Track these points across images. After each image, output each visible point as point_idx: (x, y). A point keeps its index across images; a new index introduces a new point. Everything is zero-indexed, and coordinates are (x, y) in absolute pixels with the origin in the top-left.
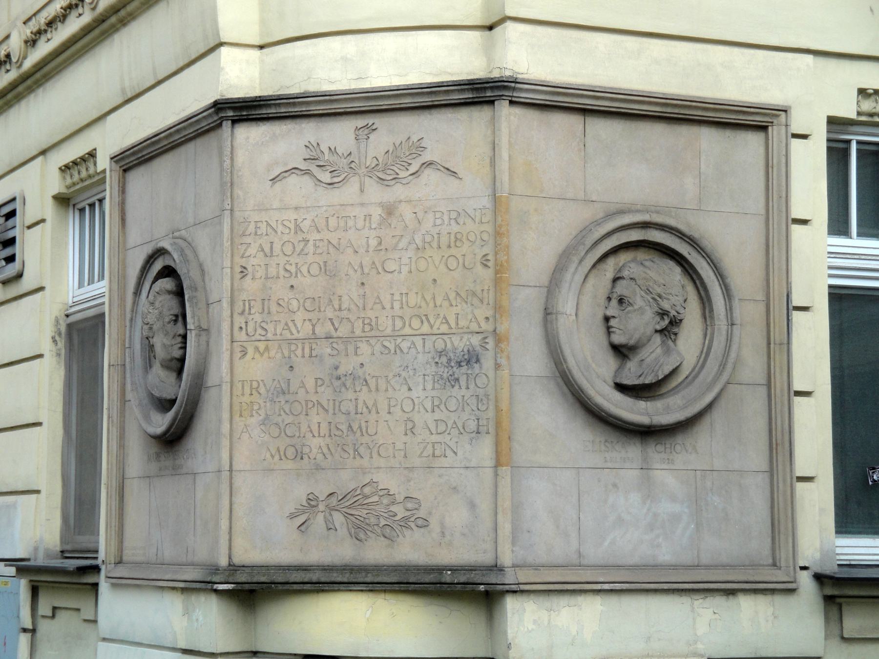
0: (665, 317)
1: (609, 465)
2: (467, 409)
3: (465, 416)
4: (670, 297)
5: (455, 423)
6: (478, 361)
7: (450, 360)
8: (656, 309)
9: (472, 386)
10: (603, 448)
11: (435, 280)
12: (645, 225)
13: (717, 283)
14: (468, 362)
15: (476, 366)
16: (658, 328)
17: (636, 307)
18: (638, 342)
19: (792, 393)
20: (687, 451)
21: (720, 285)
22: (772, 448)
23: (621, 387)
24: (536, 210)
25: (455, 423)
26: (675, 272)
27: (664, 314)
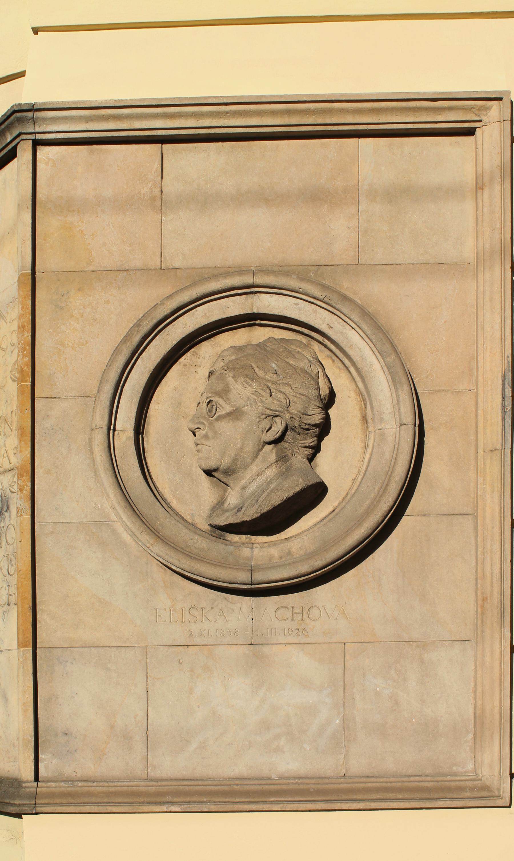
8: (260, 410)
18: (235, 461)
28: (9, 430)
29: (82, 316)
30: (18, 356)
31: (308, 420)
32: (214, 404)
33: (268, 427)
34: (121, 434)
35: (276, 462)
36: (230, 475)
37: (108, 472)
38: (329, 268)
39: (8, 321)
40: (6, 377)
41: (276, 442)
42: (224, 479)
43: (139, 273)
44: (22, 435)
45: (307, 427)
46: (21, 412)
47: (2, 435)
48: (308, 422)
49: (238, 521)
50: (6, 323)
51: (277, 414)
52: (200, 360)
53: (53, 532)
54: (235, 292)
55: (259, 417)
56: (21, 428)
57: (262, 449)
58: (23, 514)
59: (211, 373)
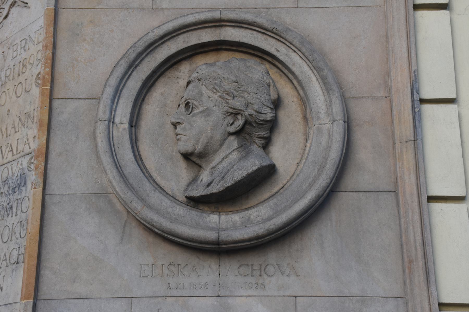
0: (239, 117)
1: (175, 293)
2: (14, 238)
3: (12, 245)
4: (245, 95)
5: (5, 255)
6: (25, 183)
7: (9, 188)
8: (226, 109)
9: (19, 212)
10: (166, 272)
11: (9, 110)
12: (217, 23)
13: (314, 79)
14: (19, 185)
15: (23, 189)
16: (232, 129)
17: (201, 109)
18: (206, 146)
19: (425, 200)
20: (283, 273)
21: (317, 80)
22: (407, 265)
23: (196, 202)
24: (91, 22)
25: (5, 255)
26: (257, 70)
27: (237, 114)
28: (31, 123)
29: (92, 40)
30: (41, 67)
31: (262, 117)
32: (190, 104)
33: (231, 121)
34: (119, 125)
35: (238, 148)
36: (202, 158)
37: (107, 154)
38: (276, 10)
39: (36, 43)
40: (32, 84)
41: (237, 133)
42: (198, 161)
43: (136, 11)
44: (41, 126)
45: (261, 122)
46: (41, 108)
47: (26, 127)
48: (262, 119)
49: (209, 193)
50: (34, 45)
51: (239, 112)
52: (181, 74)
53: (60, 202)
54: (207, 25)
55: (225, 114)
56: (41, 121)
57: (227, 139)
58: (37, 187)
59: (189, 83)
